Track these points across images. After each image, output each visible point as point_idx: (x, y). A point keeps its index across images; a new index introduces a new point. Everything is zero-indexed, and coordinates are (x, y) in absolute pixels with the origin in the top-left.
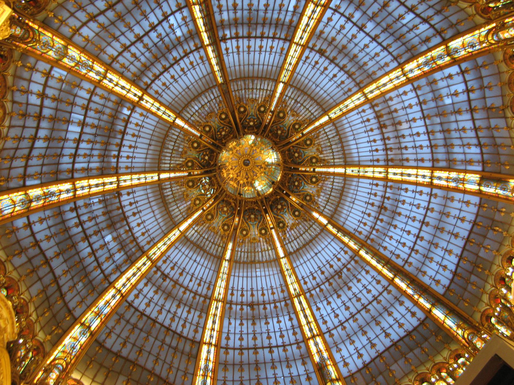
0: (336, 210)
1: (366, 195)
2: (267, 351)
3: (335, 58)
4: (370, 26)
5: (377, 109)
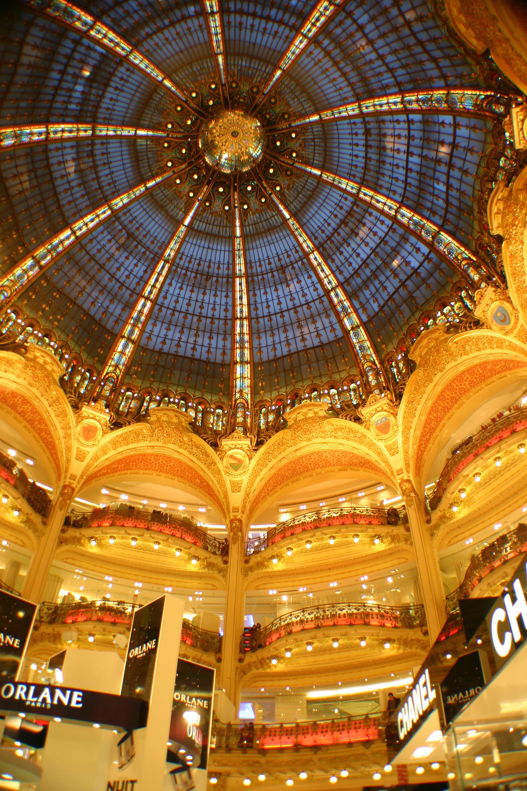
0: (254, 235)
1: (283, 249)
2: (108, 276)
3: (371, 146)
4: (415, 159)
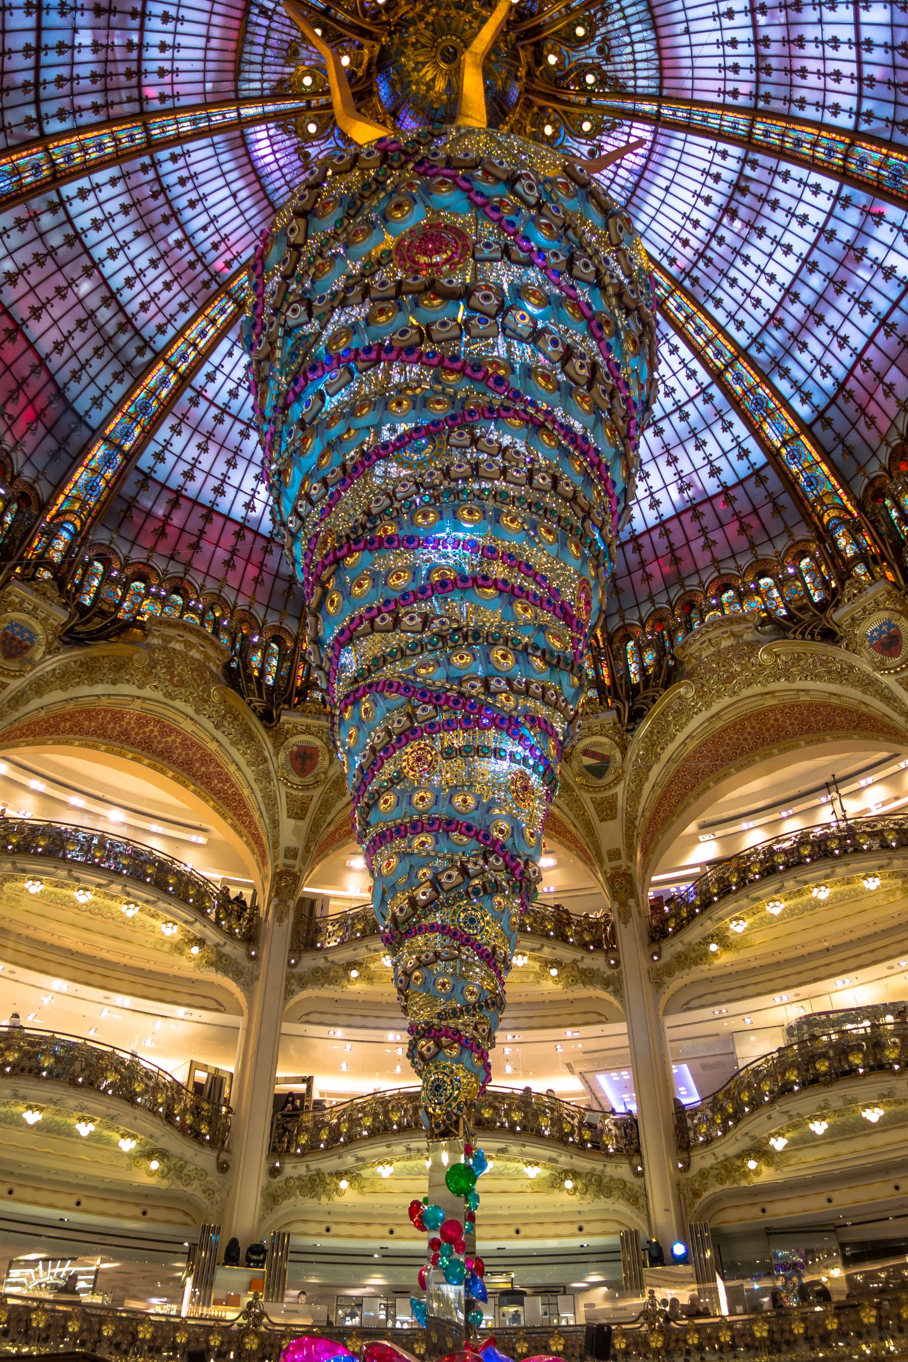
5: (748, 171)
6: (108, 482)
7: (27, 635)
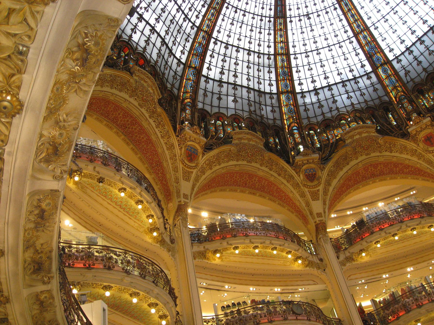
6: (293, 105)
7: (312, 170)
